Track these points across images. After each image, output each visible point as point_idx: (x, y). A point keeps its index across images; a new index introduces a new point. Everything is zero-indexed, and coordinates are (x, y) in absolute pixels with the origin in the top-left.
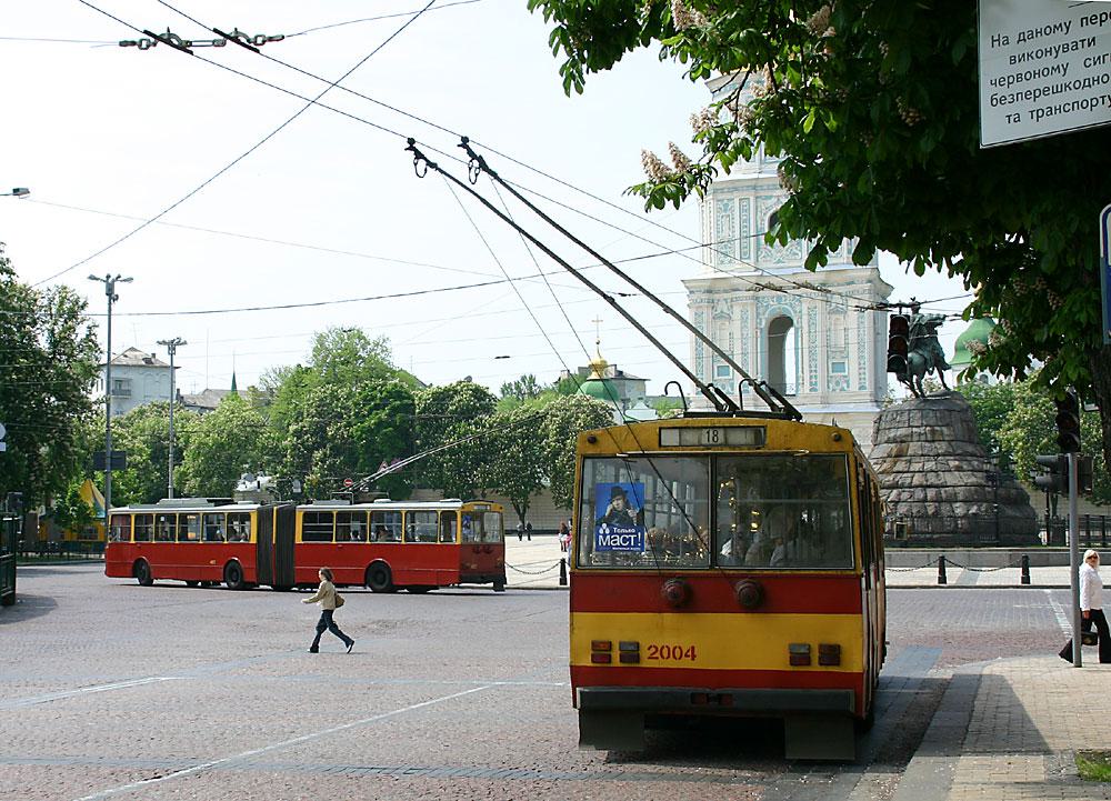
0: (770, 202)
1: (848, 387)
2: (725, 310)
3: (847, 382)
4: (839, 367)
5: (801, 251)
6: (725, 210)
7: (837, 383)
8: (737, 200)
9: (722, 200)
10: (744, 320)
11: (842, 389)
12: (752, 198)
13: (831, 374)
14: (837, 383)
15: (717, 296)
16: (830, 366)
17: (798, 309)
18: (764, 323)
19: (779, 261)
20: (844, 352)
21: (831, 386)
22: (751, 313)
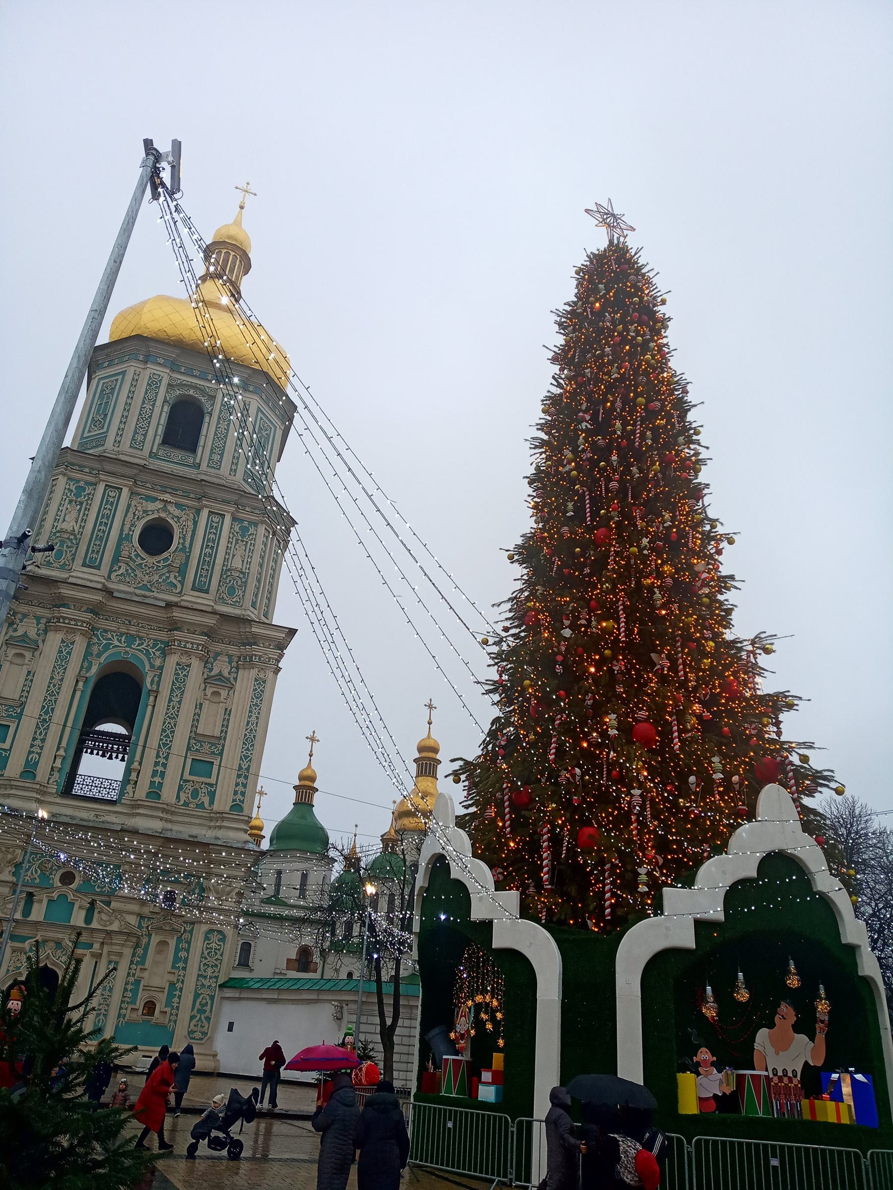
0: (151, 506)
1: (212, 802)
2: (32, 633)
3: (212, 795)
4: (202, 767)
5: (182, 583)
6: (77, 495)
7: (195, 793)
8: (101, 487)
9: (78, 481)
10: (63, 658)
11: (201, 806)
12: (125, 491)
13: (187, 776)
14: (195, 793)
15: (23, 609)
16: (189, 762)
17: (158, 663)
18: (94, 669)
19: (145, 587)
20: (218, 742)
21: (183, 797)
22: (80, 645)
